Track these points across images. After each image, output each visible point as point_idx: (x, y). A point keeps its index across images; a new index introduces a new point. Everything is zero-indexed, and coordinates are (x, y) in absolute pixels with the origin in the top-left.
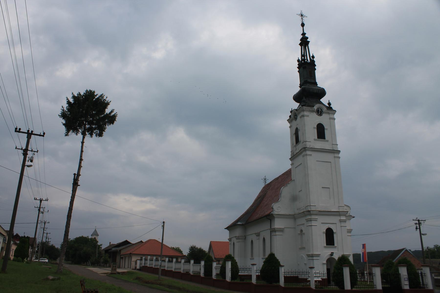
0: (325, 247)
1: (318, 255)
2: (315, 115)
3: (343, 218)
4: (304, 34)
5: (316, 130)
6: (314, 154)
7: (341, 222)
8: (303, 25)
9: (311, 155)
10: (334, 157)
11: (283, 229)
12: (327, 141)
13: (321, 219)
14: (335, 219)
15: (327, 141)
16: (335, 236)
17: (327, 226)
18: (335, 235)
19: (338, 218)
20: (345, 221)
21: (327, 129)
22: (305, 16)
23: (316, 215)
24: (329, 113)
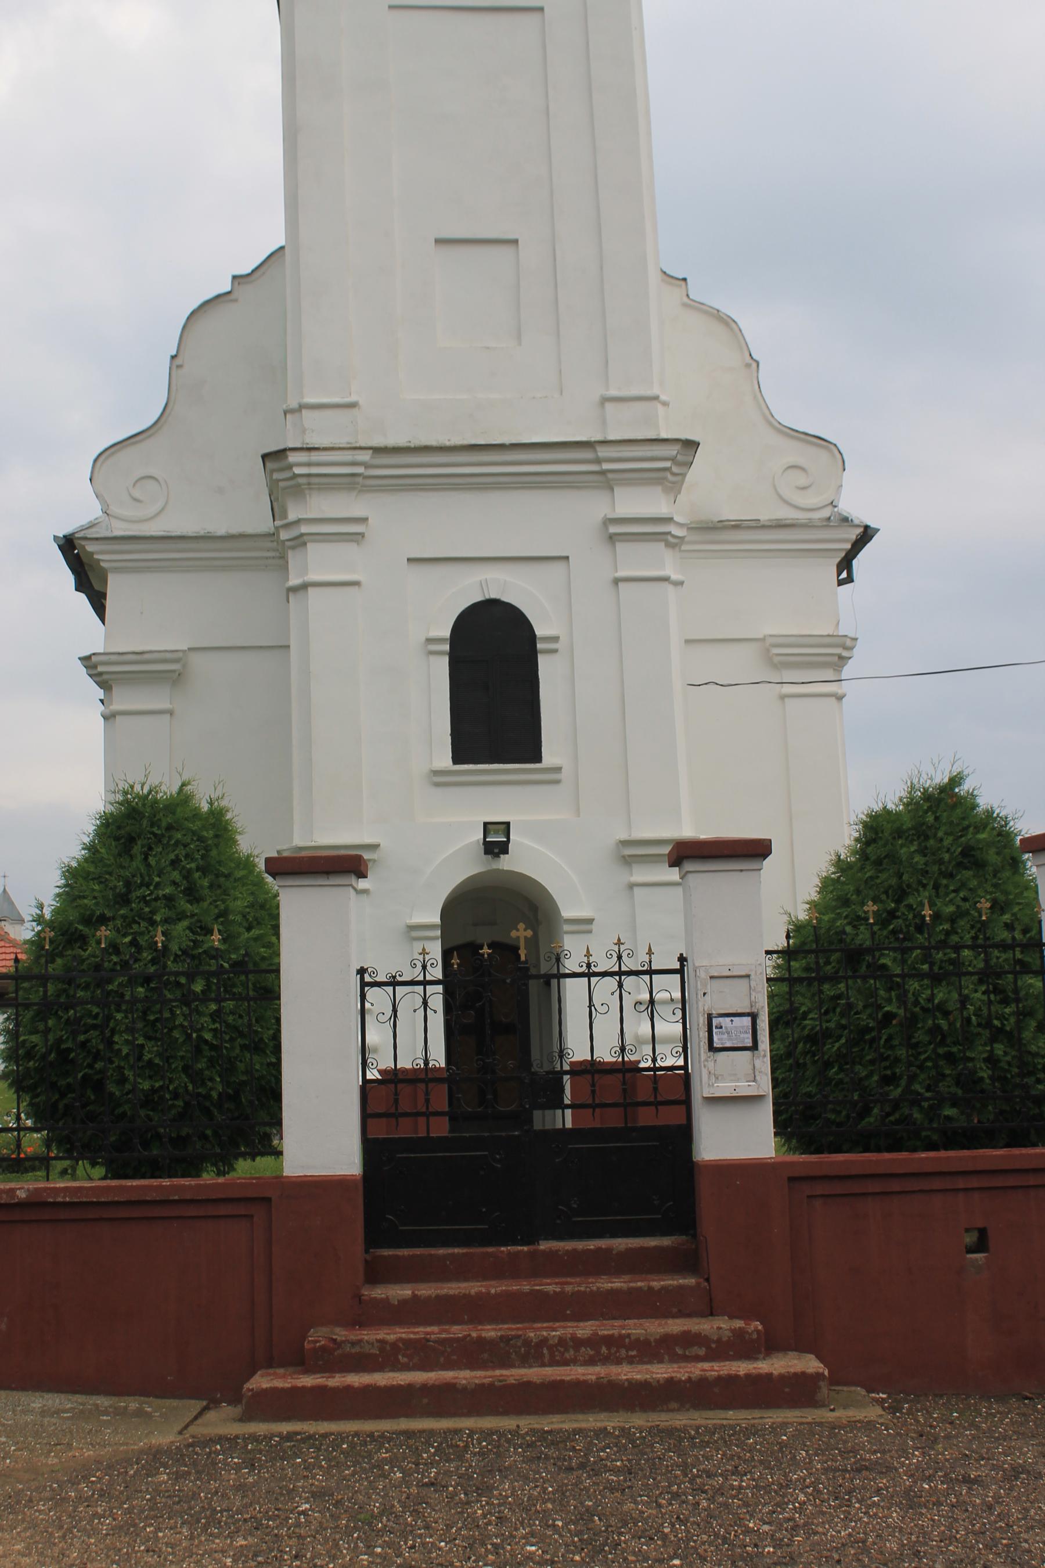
0: (438, 778)
7: (612, 539)
11: (178, 657)
13: (404, 524)
14: (564, 520)
16: (549, 671)
17: (466, 590)
18: (547, 668)
19: (592, 508)
20: (654, 532)
23: (351, 483)
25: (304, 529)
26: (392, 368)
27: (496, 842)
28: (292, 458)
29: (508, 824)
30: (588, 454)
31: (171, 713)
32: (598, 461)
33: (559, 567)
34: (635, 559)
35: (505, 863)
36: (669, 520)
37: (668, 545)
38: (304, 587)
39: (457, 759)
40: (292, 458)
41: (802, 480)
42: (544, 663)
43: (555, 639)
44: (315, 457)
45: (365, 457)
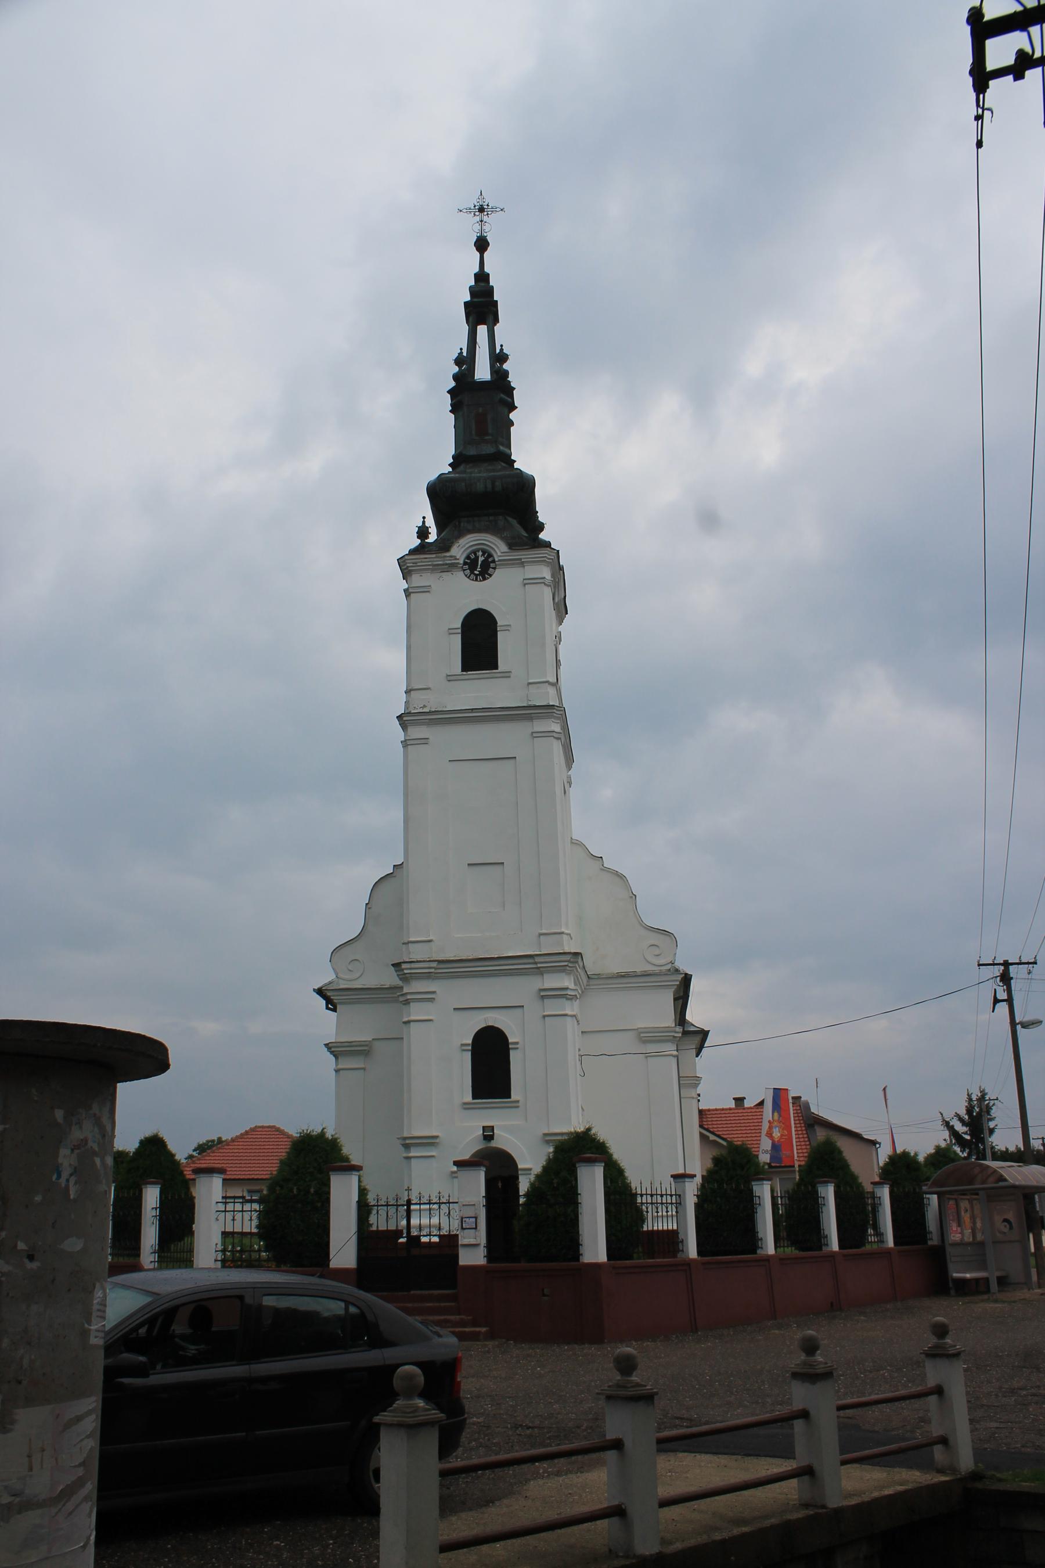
1: (430, 1142)
2: (459, 579)
3: (566, 982)
4: (482, 277)
5: (457, 640)
6: (436, 734)
8: (482, 245)
9: (425, 741)
10: (534, 735)
12: (507, 675)
13: (451, 993)
14: (520, 989)
15: (507, 675)
20: (561, 994)
21: (507, 628)
22: (494, 210)
23: (428, 976)
24: (522, 564)
25: (409, 997)
26: (446, 926)
27: (488, 1134)
28: (404, 966)
29: (493, 1127)
30: (531, 961)
31: (364, 1069)
32: (536, 963)
33: (519, 1010)
34: (553, 1007)
35: (494, 1144)
36: (567, 989)
37: (568, 999)
38: (409, 1022)
39: (474, 1098)
40: (404, 966)
41: (657, 952)
42: (512, 1054)
43: (517, 1043)
44: (413, 965)
45: (434, 965)
